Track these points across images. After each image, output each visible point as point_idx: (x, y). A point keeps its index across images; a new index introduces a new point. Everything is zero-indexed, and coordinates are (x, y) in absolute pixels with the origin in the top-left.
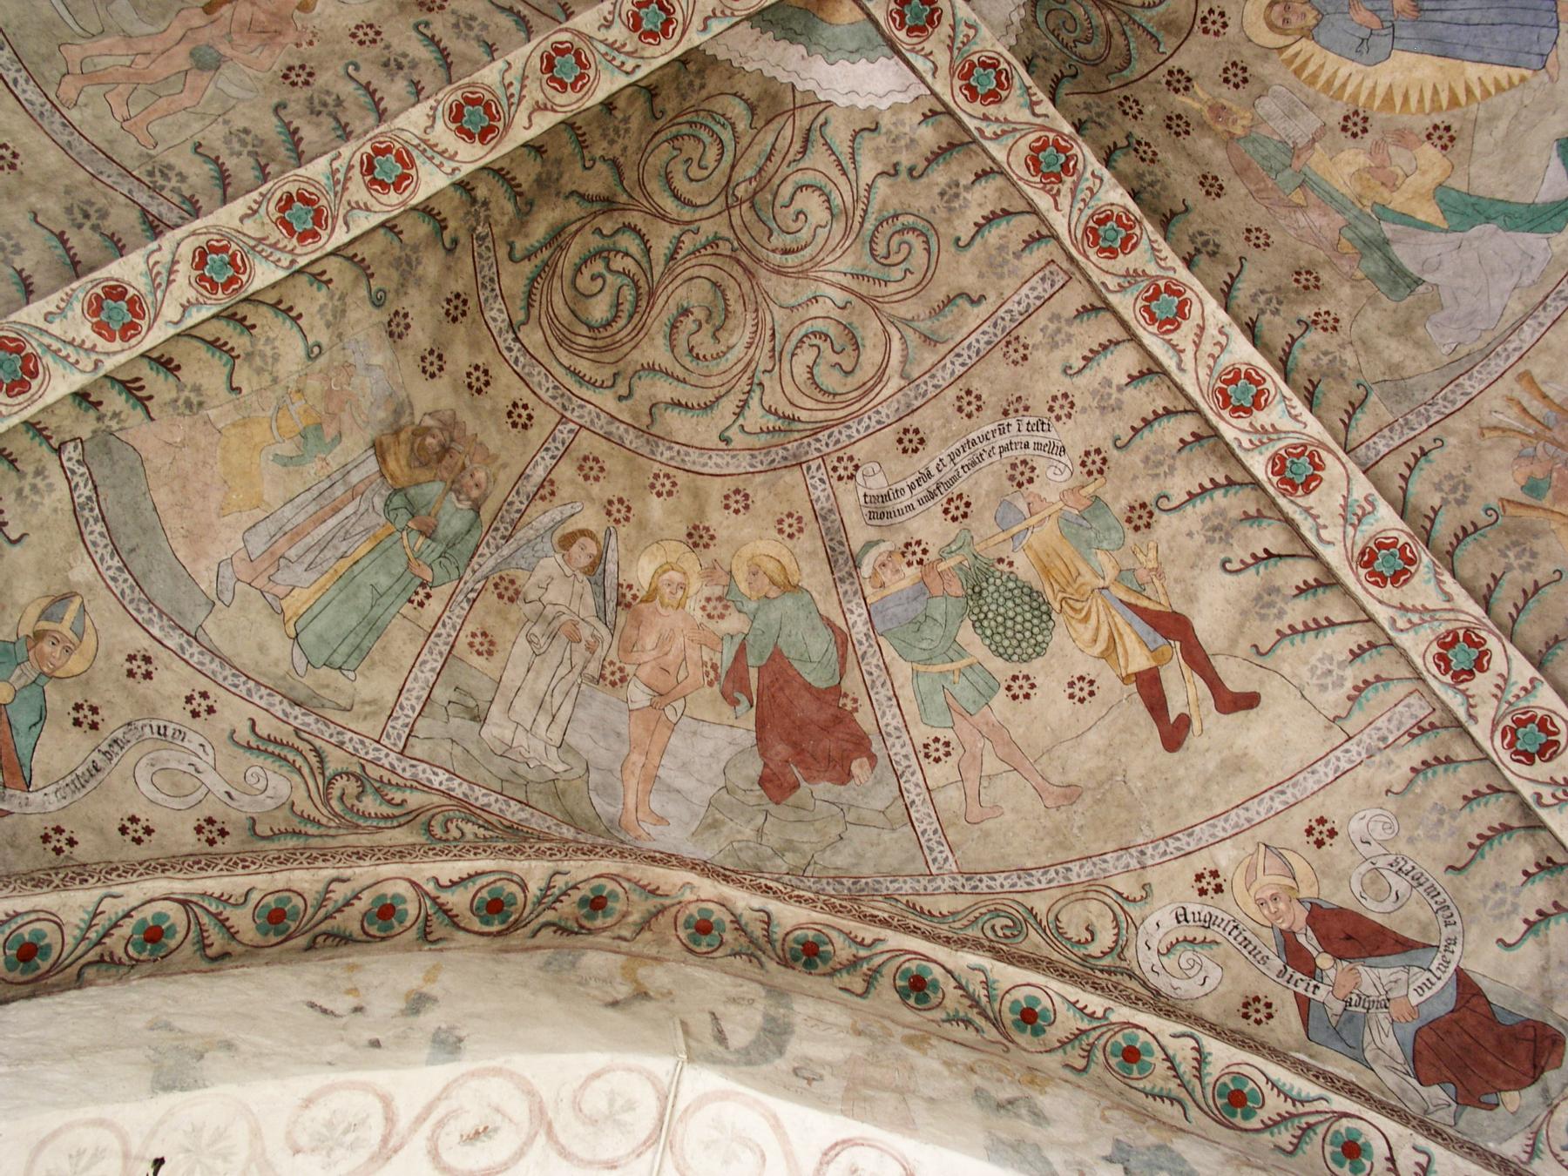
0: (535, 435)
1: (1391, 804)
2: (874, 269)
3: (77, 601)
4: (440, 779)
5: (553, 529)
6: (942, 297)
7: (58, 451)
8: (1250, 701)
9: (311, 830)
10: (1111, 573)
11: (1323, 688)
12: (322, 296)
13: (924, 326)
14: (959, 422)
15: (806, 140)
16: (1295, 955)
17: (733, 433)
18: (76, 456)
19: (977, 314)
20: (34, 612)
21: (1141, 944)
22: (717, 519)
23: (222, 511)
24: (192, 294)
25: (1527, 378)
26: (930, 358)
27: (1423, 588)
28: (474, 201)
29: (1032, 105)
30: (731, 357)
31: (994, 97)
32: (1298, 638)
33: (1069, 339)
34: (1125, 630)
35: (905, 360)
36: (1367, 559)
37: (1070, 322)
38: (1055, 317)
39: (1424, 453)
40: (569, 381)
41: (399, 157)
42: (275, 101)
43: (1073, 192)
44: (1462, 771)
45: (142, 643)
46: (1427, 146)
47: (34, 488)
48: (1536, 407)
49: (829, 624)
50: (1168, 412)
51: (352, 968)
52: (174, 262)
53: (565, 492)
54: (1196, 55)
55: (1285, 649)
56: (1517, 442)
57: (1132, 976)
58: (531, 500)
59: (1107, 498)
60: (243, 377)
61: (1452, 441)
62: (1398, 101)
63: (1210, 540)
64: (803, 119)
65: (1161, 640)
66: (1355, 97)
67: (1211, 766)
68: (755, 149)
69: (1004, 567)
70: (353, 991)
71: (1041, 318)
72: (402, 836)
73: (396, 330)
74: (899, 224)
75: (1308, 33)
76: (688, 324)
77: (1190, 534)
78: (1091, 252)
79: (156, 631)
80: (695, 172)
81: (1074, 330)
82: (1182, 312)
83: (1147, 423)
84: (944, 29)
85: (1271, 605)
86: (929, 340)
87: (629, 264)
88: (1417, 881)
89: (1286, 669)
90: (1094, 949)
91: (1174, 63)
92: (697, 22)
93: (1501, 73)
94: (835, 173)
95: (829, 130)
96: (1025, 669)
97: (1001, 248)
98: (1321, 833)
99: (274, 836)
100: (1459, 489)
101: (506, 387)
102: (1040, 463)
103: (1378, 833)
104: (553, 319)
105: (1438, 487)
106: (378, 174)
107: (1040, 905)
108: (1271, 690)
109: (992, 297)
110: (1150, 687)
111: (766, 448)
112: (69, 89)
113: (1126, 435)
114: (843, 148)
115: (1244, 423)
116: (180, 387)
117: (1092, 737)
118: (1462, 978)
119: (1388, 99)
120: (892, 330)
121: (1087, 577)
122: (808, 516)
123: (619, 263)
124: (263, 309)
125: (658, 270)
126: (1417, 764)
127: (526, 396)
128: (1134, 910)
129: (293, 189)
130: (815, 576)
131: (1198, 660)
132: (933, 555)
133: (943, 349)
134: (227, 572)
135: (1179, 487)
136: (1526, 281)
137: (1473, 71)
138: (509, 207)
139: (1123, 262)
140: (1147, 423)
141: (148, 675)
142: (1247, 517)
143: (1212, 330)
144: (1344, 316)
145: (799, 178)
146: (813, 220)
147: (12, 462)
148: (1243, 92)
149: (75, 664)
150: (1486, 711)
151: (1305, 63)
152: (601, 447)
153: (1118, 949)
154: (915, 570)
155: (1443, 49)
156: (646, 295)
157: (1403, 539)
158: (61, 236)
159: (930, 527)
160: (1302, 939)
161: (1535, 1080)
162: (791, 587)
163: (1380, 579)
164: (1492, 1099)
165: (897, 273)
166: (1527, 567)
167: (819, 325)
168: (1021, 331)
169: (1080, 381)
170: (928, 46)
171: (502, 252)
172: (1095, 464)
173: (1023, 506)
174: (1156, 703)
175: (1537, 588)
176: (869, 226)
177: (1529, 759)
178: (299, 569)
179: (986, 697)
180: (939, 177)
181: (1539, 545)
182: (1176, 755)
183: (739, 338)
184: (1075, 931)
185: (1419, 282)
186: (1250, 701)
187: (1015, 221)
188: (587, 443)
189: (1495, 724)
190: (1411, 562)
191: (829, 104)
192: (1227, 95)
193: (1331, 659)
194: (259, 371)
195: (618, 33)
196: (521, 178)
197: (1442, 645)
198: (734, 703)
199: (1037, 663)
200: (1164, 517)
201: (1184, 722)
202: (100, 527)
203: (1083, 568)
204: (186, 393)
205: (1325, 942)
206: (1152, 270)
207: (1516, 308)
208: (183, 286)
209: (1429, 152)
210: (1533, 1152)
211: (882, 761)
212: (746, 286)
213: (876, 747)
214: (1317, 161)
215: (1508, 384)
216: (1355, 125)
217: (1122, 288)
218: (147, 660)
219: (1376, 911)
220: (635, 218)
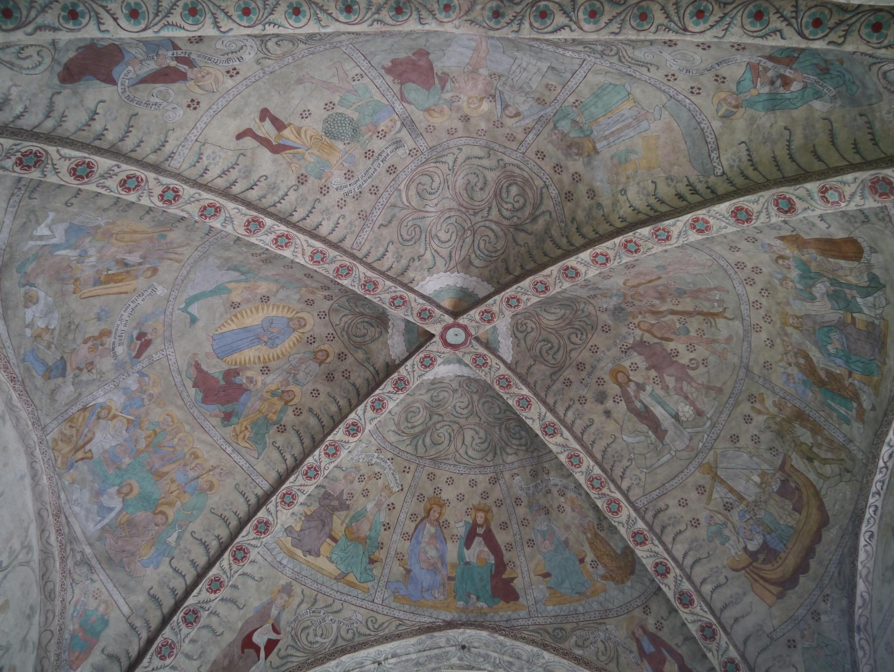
0: (534, 149)
1: (170, 126)
2: (418, 222)
3: (720, 114)
5: (524, 118)
6: (393, 222)
7: (724, 173)
8: (239, 137)
10: (307, 156)
11: (214, 153)
12: (622, 213)
13: (397, 210)
14: (376, 183)
15: (450, 257)
16: (188, 61)
17: (456, 152)
18: (717, 170)
19: (380, 221)
20: (738, 115)
21: (255, 46)
22: (459, 125)
23: (658, 137)
24: (672, 228)
26: (392, 200)
27: (194, 210)
28: (567, 237)
29: (381, 299)
30: (462, 176)
31: (394, 298)
32: (230, 165)
33: (346, 228)
34: (295, 139)
35: (400, 196)
36: (218, 210)
37: (348, 233)
38: (353, 232)
40: (523, 166)
41: (597, 262)
43: (360, 279)
44: (148, 150)
45: (693, 98)
46: (239, 301)
47: (734, 161)
49: (409, 103)
50: (305, 219)
52: (678, 238)
53: (520, 130)
54: (326, 305)
55: (233, 160)
58: (533, 128)
59: (316, 181)
60: (651, 187)
62: (254, 310)
63: (274, 183)
64: (453, 263)
65: (281, 142)
66: (268, 307)
67: (247, 110)
68: (467, 248)
69: (346, 142)
71: (357, 230)
73: (592, 193)
74: (414, 241)
75: (291, 319)
76: (480, 185)
77: (282, 181)
78: (348, 264)
79: (688, 101)
80: (487, 239)
81: (345, 231)
82: (312, 258)
83: (311, 212)
84: (415, 312)
85: (244, 173)
86: (394, 206)
87: (506, 206)
89: (230, 153)
91: (331, 302)
92: (498, 302)
93: (224, 330)
94: (439, 250)
95: (444, 262)
96: (330, 113)
97: (378, 247)
98: (194, 104)
101: (547, 166)
102: (343, 181)
103: (171, 114)
104: (531, 189)
106: (604, 258)
108: (233, 144)
109: (376, 229)
110: (279, 125)
111: (444, 150)
112: (709, 263)
113: (317, 205)
114: (438, 259)
115: (278, 233)
116: (675, 187)
117: (297, 102)
118: (113, 82)
119: (257, 309)
120: (407, 204)
121: (315, 151)
123: (509, 206)
124: (644, 211)
125: (494, 203)
126: (167, 145)
127: (539, 162)
128: (262, 55)
129: (634, 254)
130: (418, 116)
131: (265, 142)
132: (375, 137)
133: (388, 205)
134: (657, 116)
135: (293, 196)
137: (233, 327)
138: (553, 233)
139: (337, 264)
140: (311, 212)
141: (692, 88)
142: (264, 197)
143: (300, 255)
145: (450, 243)
146: (443, 231)
147: (742, 173)
148: (306, 299)
149: (723, 95)
150: (152, 183)
151: (288, 311)
152: (508, 144)
154: (380, 129)
155: (245, 329)
156: (497, 194)
157: (208, 220)
159: (378, 145)
160: (186, 67)
162: (427, 110)
163: (210, 205)
164: (80, 51)
165: (410, 224)
167: (433, 197)
168: (363, 222)
169: (338, 215)
170: (419, 306)
171: (554, 215)
172: (324, 190)
173: (346, 165)
176: (423, 236)
177: (128, 177)
178: (627, 115)
179: (342, 98)
180: (404, 262)
182: (262, 107)
183: (460, 182)
186: (239, 137)
187: (376, 258)
188: (514, 146)
189: (147, 181)
190: (202, 215)
191: (445, 272)
192: (311, 297)
193: (215, 164)
194: (644, 188)
195: (524, 298)
196: (550, 243)
197: (178, 196)
198: (443, 73)
199: (326, 116)
200: (294, 183)
201: (262, 119)
202: (709, 140)
203: (318, 153)
204: (673, 184)
205: (176, 70)
206: (326, 266)
208: (675, 231)
209: (237, 299)
212: (461, 200)
213: (383, 72)
214: (274, 287)
216: (265, 299)
217: (335, 257)
218: (692, 93)
219: (160, 87)
220: (506, 222)
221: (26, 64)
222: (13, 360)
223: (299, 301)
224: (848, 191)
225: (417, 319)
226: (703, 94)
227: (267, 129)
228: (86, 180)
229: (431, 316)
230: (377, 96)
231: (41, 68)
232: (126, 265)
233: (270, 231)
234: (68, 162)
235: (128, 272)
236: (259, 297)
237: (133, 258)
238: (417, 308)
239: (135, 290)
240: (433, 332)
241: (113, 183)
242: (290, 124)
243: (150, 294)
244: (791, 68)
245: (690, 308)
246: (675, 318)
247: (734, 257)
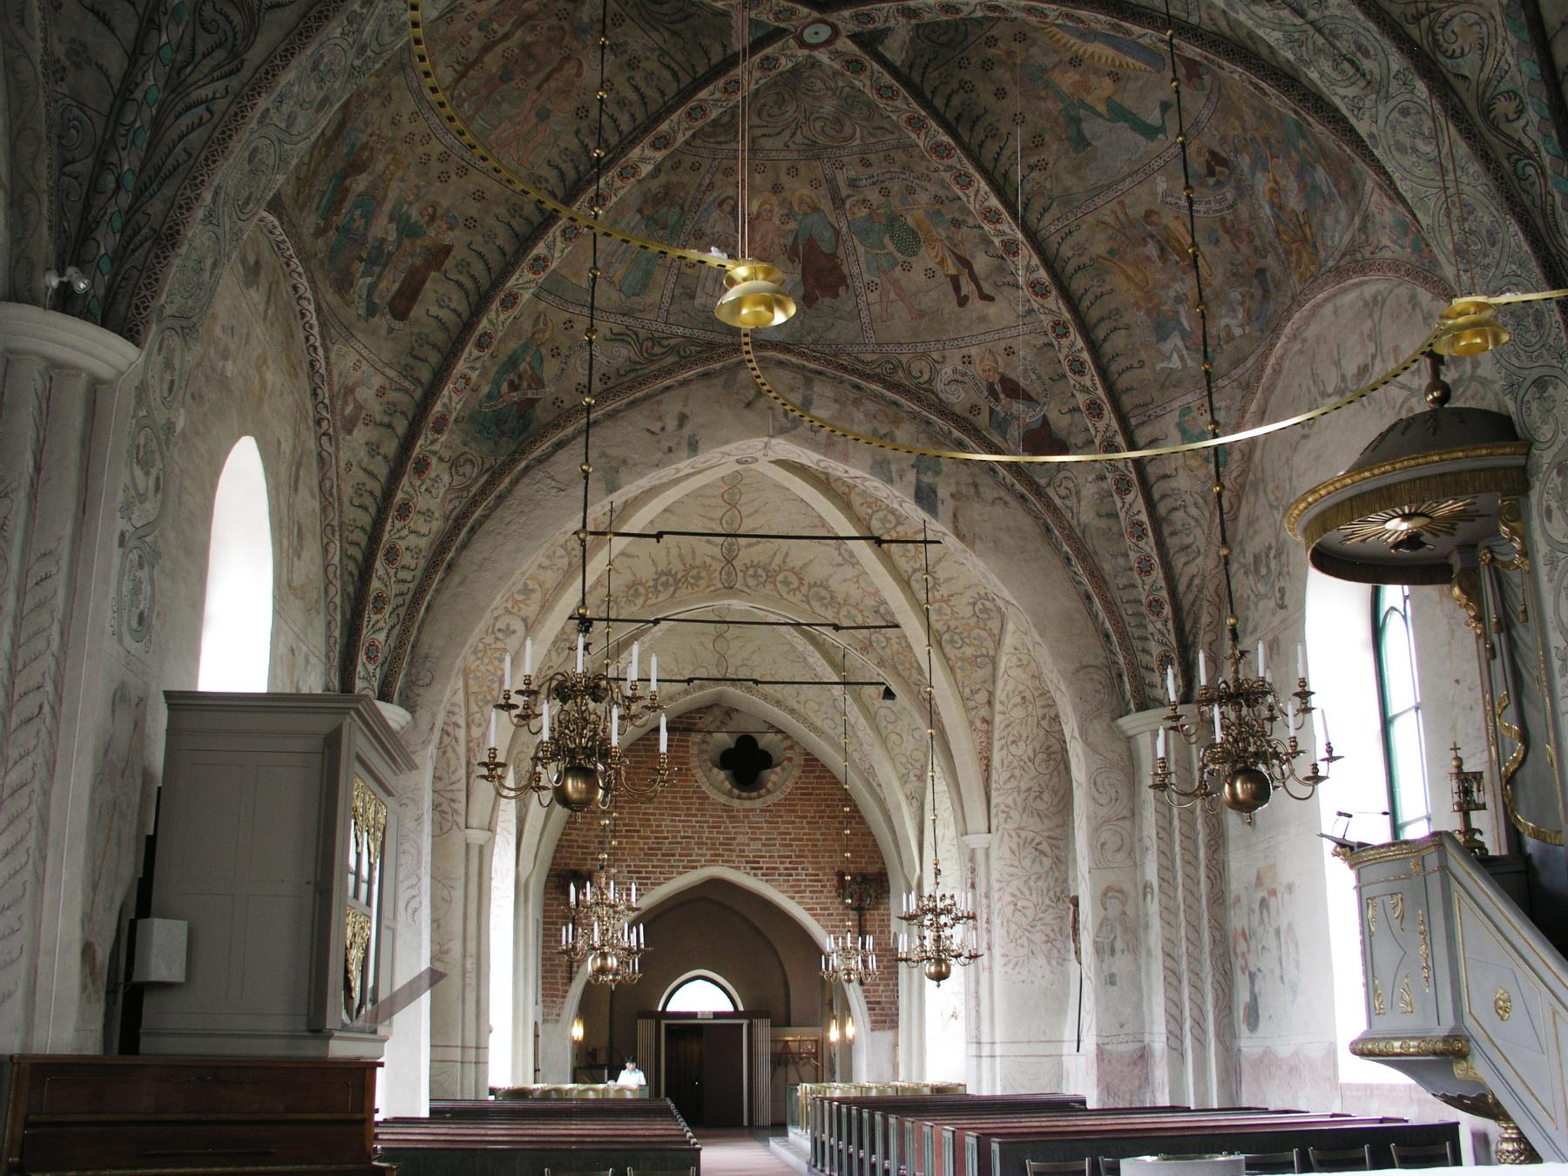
4: (680, 331)
5: (714, 201)
8: (991, 299)
9: (638, 367)
10: (944, 236)
17: (790, 143)
22: (785, 180)
25: (1121, 203)
30: (787, 115)
31: (891, 98)
39: (1070, 232)
42: (575, 129)
45: (567, 316)
48: (1122, 217)
49: (832, 226)
55: (1005, 288)
56: (1110, 231)
57: (933, 393)
58: (704, 193)
61: (1084, 227)
66: (1077, 51)
70: (660, 418)
72: (670, 360)
84: (868, 73)
88: (1039, 378)
90: (921, 380)
92: (753, 82)
93: (1143, 66)
96: (909, 259)
98: (1010, 352)
99: (627, 373)
100: (1080, 249)
105: (1072, 248)
107: (904, 360)
108: (998, 298)
111: (805, 151)
118: (1045, 418)
122: (823, 180)
128: (938, 366)
130: (826, 205)
132: (874, 207)
136: (1133, 158)
137: (1130, 60)
139: (946, 162)
143: (982, 192)
144: (1051, 161)
149: (548, 335)
150: (1065, 351)
153: (930, 381)
158: (509, 225)
159: (873, 196)
162: (816, 209)
166: (1099, 286)
174: (957, 289)
175: (1102, 295)
181: (1107, 277)
184: (916, 373)
185: (1089, 144)
192: (1015, 46)
201: (966, 298)
205: (1004, 390)
206: (959, 166)
207: (1126, 170)
209: (1107, 82)
210: (1049, 485)
211: (851, 288)
214: (1056, 76)
215: (1113, 205)
216: (1076, 62)
219: (1022, 383)
221: (1071, 485)
222: (1260, 350)
223: (1034, 43)
225: (867, 63)
226: (561, 325)
227: (967, 287)
229: (848, 62)
230: (861, 249)
231: (1068, 474)
232: (1162, 250)
233: (1000, 233)
234: (1097, 424)
235: (1167, 241)
236: (1081, 69)
237: (1151, 249)
238: (865, 77)
239: (1177, 218)
240: (849, 42)
241: (1087, 381)
242: (946, 276)
243: (1172, 196)
244: (515, 403)
245: (488, 59)
246: (501, 31)
247: (475, 180)
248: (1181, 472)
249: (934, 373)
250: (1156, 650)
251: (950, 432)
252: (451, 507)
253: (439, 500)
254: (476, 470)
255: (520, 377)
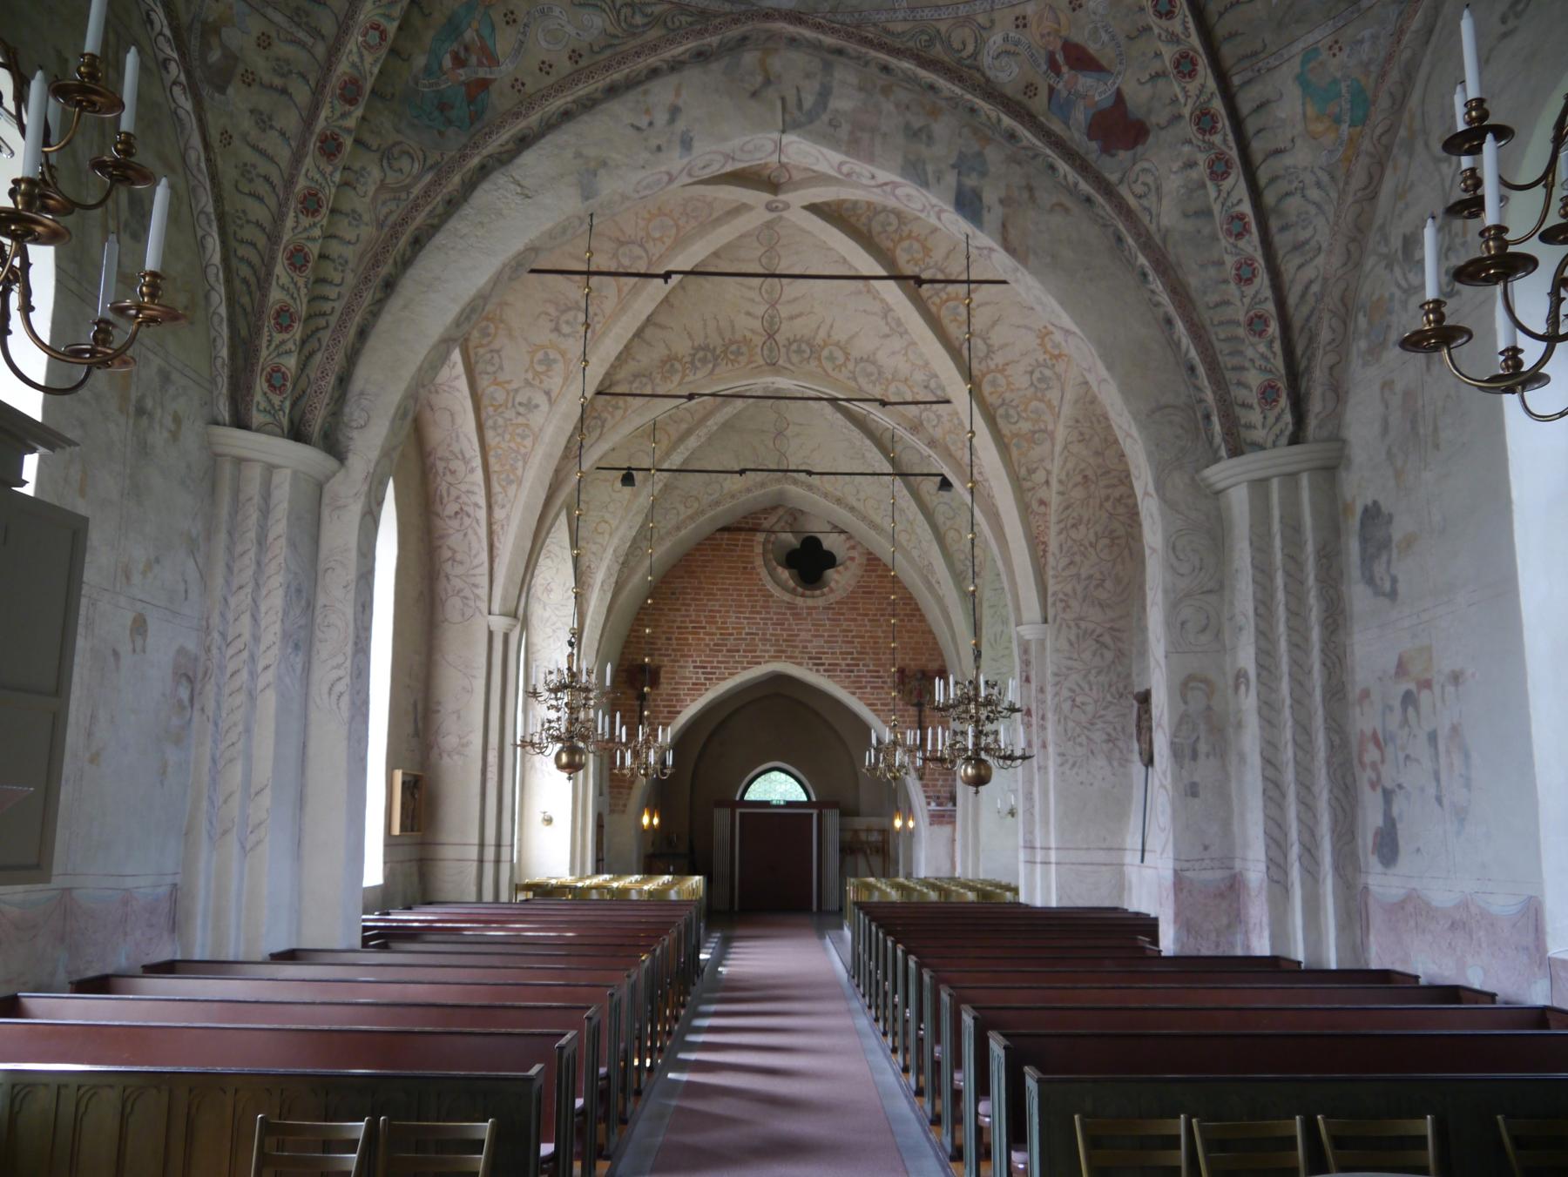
9: (616, 42)
16: (1053, 66)
21: (986, 53)
51: (646, 93)
57: (978, 70)
70: (647, 112)
72: (654, 34)
88: (1113, 38)
90: (965, 54)
99: (603, 49)
107: (943, 27)
118: (1119, 95)
128: (985, 34)
153: (974, 55)
160: (1057, 56)
161: (1133, 148)
184: (957, 45)
205: (1067, 58)
210: (1121, 181)
219: (1092, 48)
221: (1149, 179)
224: (369, 59)
228: (1191, 53)
231: (1146, 165)
234: (1189, 87)
244: (463, 83)
248: (1299, 142)
249: (980, 42)
250: (1255, 379)
251: (999, 120)
252: (385, 210)
253: (367, 200)
254: (416, 165)
255: (467, 49)
